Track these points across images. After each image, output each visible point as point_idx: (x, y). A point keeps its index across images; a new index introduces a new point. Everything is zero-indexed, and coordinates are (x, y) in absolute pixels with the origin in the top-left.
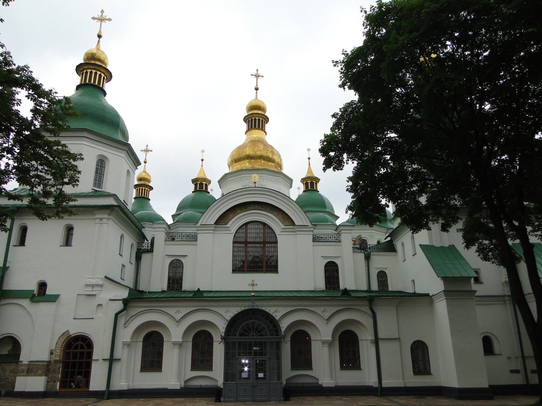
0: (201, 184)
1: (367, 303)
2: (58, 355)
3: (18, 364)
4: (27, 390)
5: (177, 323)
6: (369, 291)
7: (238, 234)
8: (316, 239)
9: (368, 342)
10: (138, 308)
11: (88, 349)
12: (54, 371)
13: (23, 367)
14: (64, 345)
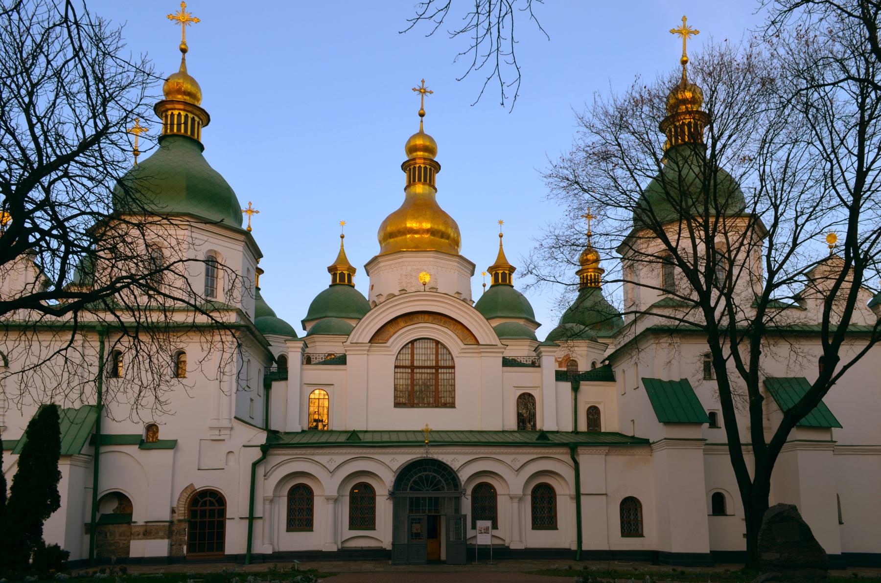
0: (342, 274)
1: (569, 451)
3: (130, 525)
4: (146, 556)
5: (331, 475)
7: (401, 356)
10: (280, 457)
11: (219, 505)
14: (188, 502)
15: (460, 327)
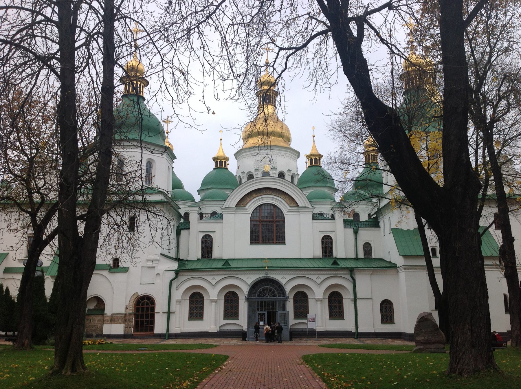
0: (221, 162)
1: (349, 272)
2: (131, 309)
4: (112, 333)
6: (356, 259)
8: (315, 217)
9: (350, 300)
11: (151, 305)
12: (129, 321)
13: (108, 318)
15: (287, 197)
